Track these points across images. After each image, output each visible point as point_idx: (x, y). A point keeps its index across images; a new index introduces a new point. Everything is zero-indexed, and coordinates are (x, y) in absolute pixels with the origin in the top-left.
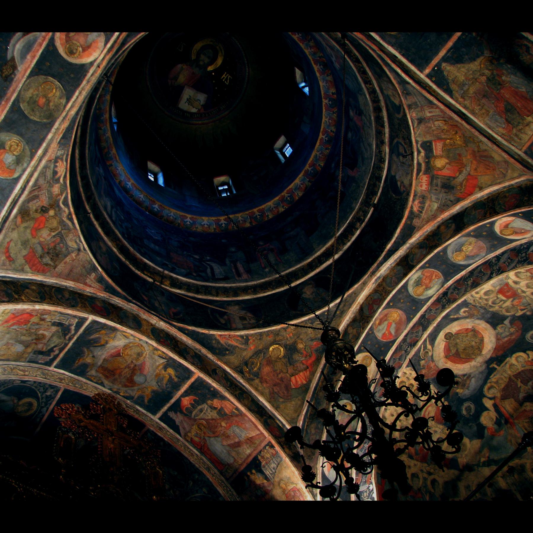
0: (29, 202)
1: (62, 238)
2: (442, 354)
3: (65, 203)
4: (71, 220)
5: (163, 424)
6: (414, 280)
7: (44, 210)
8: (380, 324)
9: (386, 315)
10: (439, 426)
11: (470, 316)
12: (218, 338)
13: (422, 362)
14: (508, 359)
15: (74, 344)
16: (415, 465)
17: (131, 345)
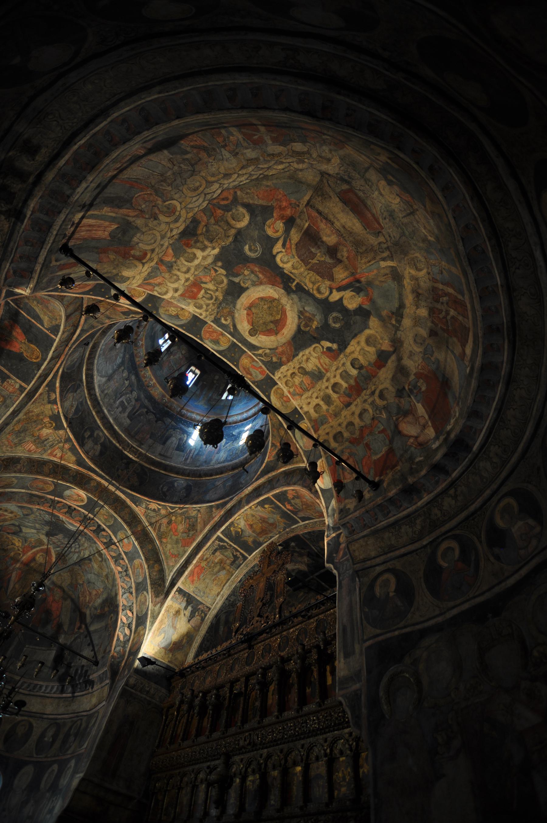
0: (159, 531)
1: (188, 518)
2: (273, 338)
3: (172, 508)
4: (183, 508)
5: (307, 522)
6: (213, 346)
7: (170, 523)
8: (251, 375)
9: (244, 369)
10: (340, 359)
11: (231, 314)
12: (269, 460)
13: (275, 360)
14: (285, 271)
15: (235, 544)
16: (356, 405)
17: (245, 518)
